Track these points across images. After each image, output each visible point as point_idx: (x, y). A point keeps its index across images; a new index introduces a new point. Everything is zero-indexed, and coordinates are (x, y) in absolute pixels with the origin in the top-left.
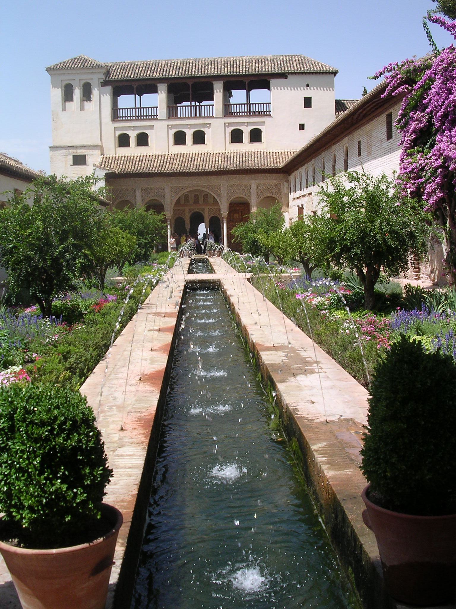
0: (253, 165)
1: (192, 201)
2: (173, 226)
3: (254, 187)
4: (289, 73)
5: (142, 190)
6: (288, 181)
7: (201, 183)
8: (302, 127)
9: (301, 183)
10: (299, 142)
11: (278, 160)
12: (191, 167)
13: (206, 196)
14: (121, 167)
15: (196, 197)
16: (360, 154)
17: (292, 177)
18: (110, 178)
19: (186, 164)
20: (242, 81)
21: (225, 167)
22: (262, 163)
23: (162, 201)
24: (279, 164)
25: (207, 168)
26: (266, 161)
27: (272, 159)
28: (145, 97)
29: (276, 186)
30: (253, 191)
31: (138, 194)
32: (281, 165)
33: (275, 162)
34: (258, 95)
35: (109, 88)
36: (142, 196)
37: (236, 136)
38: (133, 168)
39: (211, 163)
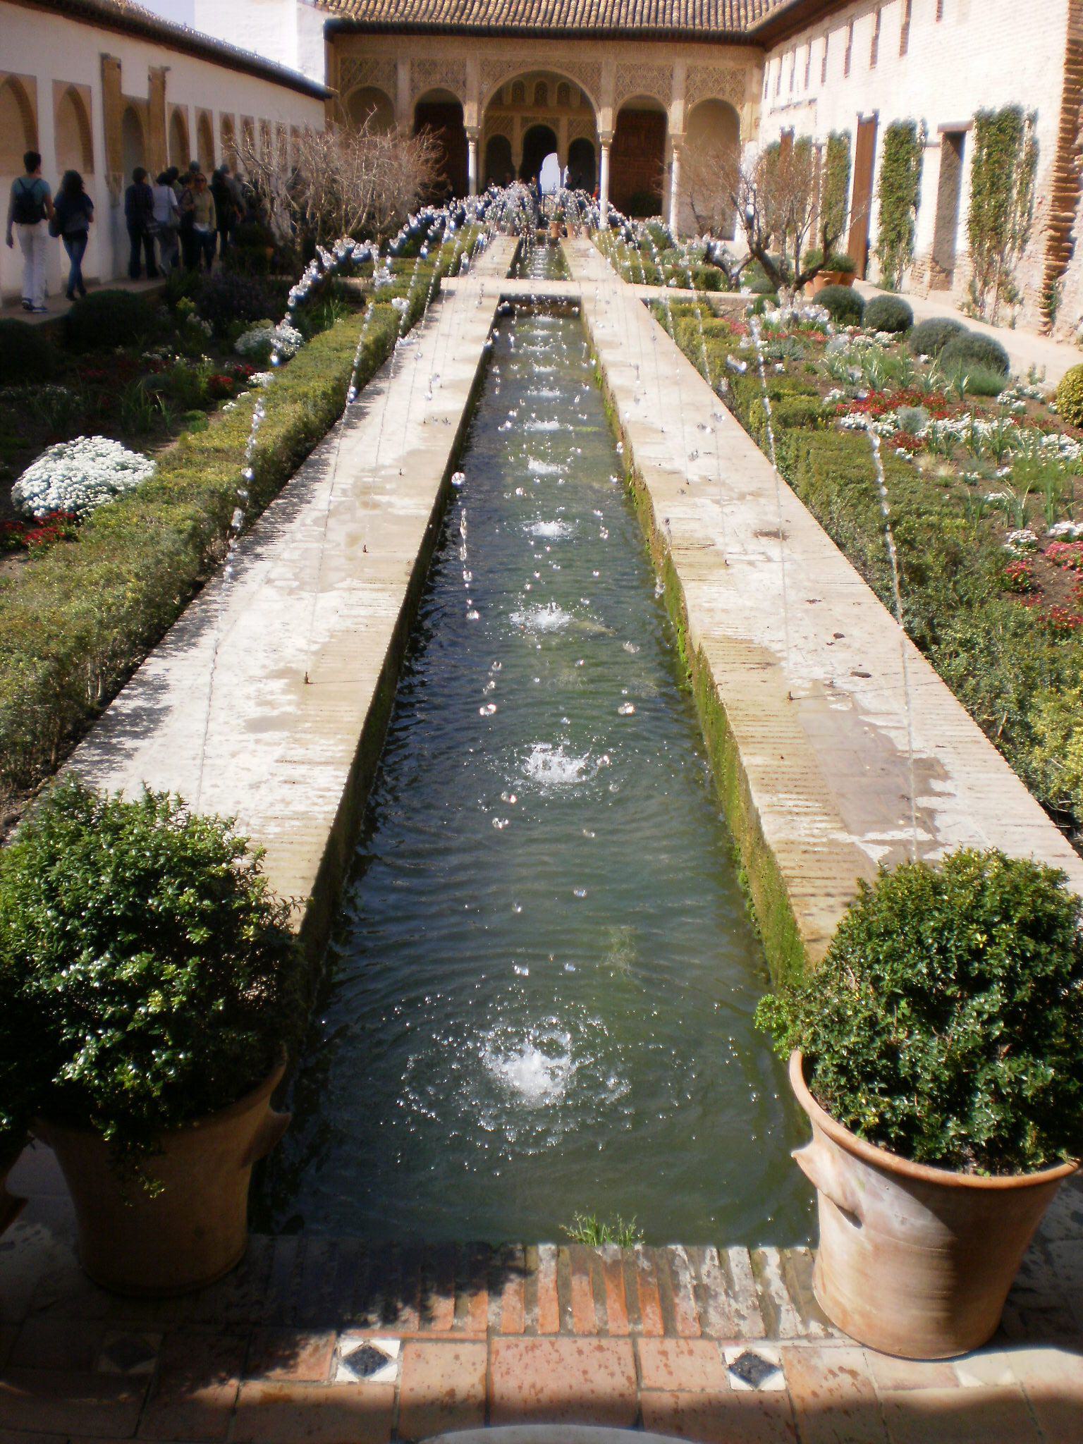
0: (682, 20)
1: (530, 97)
2: (483, 156)
3: (679, 75)
5: (413, 65)
6: (761, 67)
7: (555, 58)
9: (793, 71)
11: (742, 12)
12: (533, 16)
14: (363, 7)
15: (542, 90)
19: (521, 8)
21: (614, 19)
22: (705, 17)
23: (459, 95)
24: (743, 22)
25: (570, 19)
26: (713, 12)
27: (727, 9)
29: (733, 75)
31: (404, 76)
32: (751, 26)
33: (735, 16)
36: (412, 80)
38: (392, 10)
39: (580, 9)
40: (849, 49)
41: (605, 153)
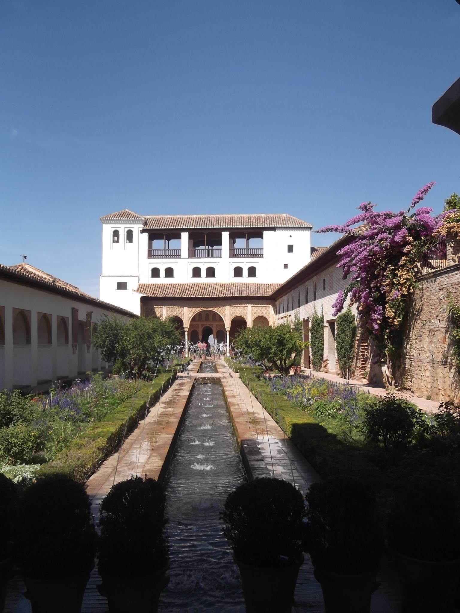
1: (204, 319)
2: (190, 336)
4: (277, 227)
8: (286, 266)
10: (283, 277)
13: (215, 315)
15: (207, 315)
16: (324, 289)
17: (277, 303)
18: (143, 299)
20: (243, 232)
23: (182, 318)
28: (172, 241)
30: (249, 313)
34: (254, 242)
35: (146, 235)
37: (238, 272)
40: (299, 300)
41: (228, 334)
